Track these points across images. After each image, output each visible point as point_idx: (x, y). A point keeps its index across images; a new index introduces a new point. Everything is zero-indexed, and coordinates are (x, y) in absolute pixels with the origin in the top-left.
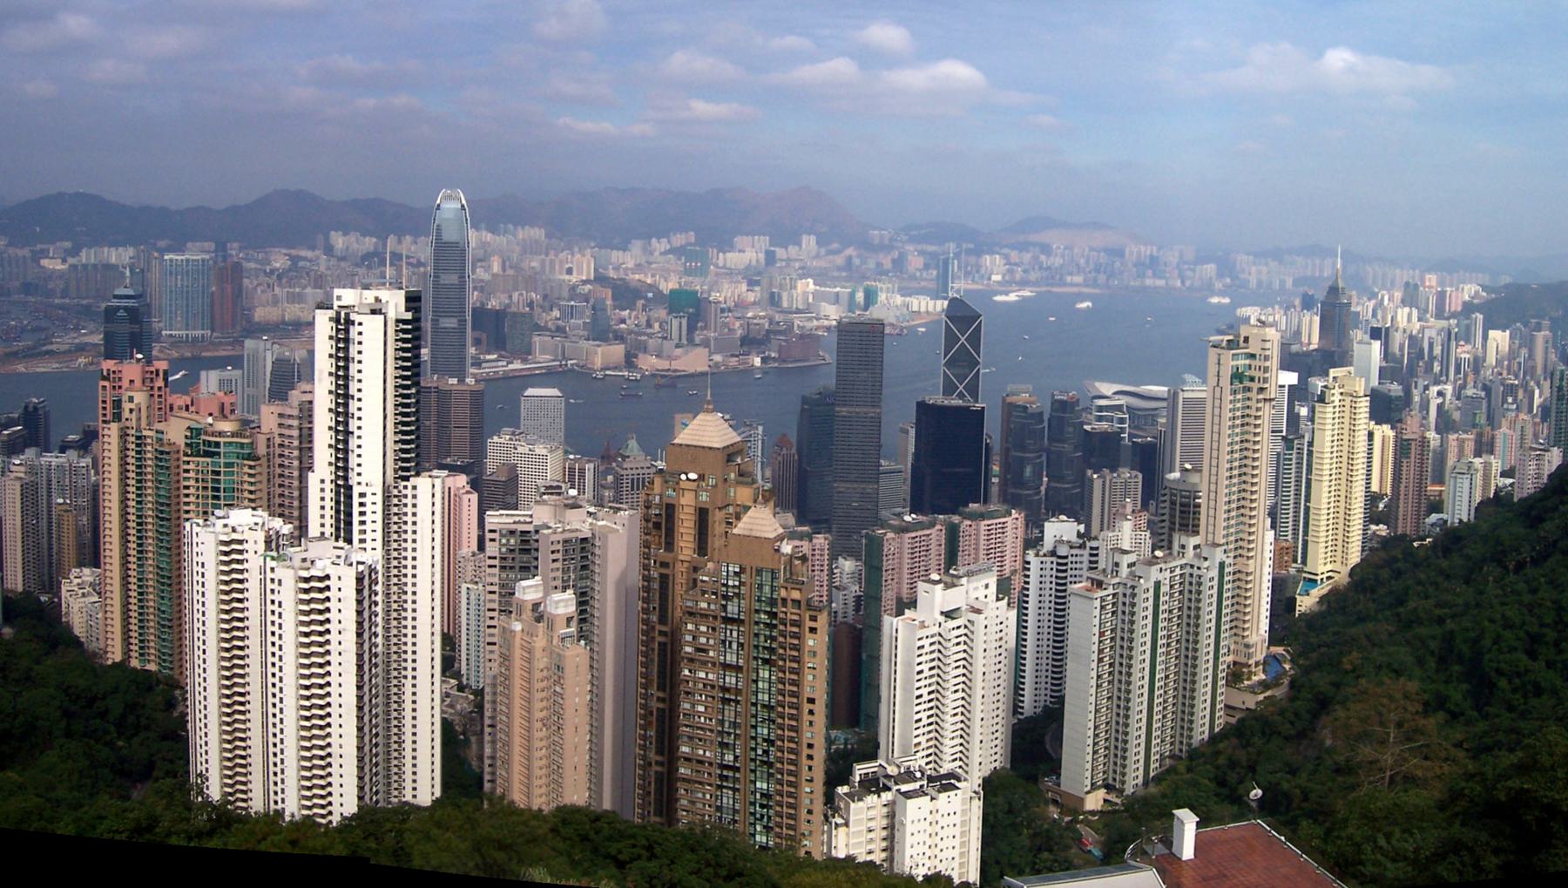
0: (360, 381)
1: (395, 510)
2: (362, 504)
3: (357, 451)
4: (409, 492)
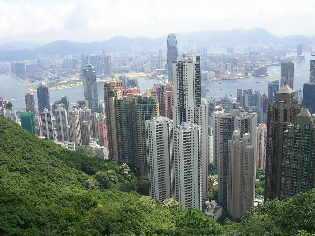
0: (187, 81)
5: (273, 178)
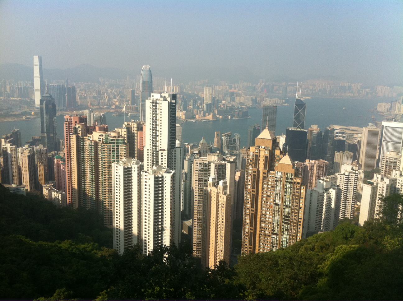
1: (170, 157)
2: (162, 156)
3: (160, 141)
4: (174, 152)
5: (251, 229)
